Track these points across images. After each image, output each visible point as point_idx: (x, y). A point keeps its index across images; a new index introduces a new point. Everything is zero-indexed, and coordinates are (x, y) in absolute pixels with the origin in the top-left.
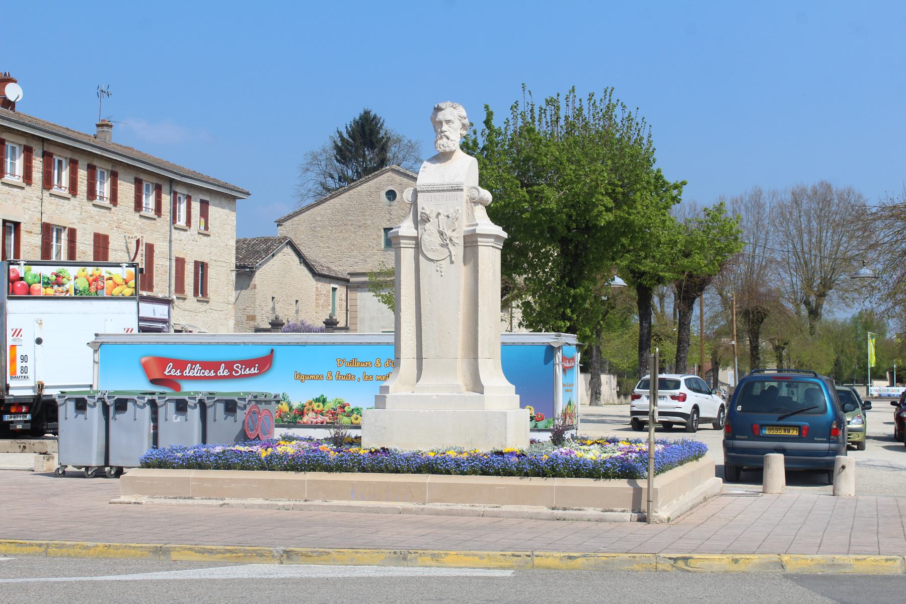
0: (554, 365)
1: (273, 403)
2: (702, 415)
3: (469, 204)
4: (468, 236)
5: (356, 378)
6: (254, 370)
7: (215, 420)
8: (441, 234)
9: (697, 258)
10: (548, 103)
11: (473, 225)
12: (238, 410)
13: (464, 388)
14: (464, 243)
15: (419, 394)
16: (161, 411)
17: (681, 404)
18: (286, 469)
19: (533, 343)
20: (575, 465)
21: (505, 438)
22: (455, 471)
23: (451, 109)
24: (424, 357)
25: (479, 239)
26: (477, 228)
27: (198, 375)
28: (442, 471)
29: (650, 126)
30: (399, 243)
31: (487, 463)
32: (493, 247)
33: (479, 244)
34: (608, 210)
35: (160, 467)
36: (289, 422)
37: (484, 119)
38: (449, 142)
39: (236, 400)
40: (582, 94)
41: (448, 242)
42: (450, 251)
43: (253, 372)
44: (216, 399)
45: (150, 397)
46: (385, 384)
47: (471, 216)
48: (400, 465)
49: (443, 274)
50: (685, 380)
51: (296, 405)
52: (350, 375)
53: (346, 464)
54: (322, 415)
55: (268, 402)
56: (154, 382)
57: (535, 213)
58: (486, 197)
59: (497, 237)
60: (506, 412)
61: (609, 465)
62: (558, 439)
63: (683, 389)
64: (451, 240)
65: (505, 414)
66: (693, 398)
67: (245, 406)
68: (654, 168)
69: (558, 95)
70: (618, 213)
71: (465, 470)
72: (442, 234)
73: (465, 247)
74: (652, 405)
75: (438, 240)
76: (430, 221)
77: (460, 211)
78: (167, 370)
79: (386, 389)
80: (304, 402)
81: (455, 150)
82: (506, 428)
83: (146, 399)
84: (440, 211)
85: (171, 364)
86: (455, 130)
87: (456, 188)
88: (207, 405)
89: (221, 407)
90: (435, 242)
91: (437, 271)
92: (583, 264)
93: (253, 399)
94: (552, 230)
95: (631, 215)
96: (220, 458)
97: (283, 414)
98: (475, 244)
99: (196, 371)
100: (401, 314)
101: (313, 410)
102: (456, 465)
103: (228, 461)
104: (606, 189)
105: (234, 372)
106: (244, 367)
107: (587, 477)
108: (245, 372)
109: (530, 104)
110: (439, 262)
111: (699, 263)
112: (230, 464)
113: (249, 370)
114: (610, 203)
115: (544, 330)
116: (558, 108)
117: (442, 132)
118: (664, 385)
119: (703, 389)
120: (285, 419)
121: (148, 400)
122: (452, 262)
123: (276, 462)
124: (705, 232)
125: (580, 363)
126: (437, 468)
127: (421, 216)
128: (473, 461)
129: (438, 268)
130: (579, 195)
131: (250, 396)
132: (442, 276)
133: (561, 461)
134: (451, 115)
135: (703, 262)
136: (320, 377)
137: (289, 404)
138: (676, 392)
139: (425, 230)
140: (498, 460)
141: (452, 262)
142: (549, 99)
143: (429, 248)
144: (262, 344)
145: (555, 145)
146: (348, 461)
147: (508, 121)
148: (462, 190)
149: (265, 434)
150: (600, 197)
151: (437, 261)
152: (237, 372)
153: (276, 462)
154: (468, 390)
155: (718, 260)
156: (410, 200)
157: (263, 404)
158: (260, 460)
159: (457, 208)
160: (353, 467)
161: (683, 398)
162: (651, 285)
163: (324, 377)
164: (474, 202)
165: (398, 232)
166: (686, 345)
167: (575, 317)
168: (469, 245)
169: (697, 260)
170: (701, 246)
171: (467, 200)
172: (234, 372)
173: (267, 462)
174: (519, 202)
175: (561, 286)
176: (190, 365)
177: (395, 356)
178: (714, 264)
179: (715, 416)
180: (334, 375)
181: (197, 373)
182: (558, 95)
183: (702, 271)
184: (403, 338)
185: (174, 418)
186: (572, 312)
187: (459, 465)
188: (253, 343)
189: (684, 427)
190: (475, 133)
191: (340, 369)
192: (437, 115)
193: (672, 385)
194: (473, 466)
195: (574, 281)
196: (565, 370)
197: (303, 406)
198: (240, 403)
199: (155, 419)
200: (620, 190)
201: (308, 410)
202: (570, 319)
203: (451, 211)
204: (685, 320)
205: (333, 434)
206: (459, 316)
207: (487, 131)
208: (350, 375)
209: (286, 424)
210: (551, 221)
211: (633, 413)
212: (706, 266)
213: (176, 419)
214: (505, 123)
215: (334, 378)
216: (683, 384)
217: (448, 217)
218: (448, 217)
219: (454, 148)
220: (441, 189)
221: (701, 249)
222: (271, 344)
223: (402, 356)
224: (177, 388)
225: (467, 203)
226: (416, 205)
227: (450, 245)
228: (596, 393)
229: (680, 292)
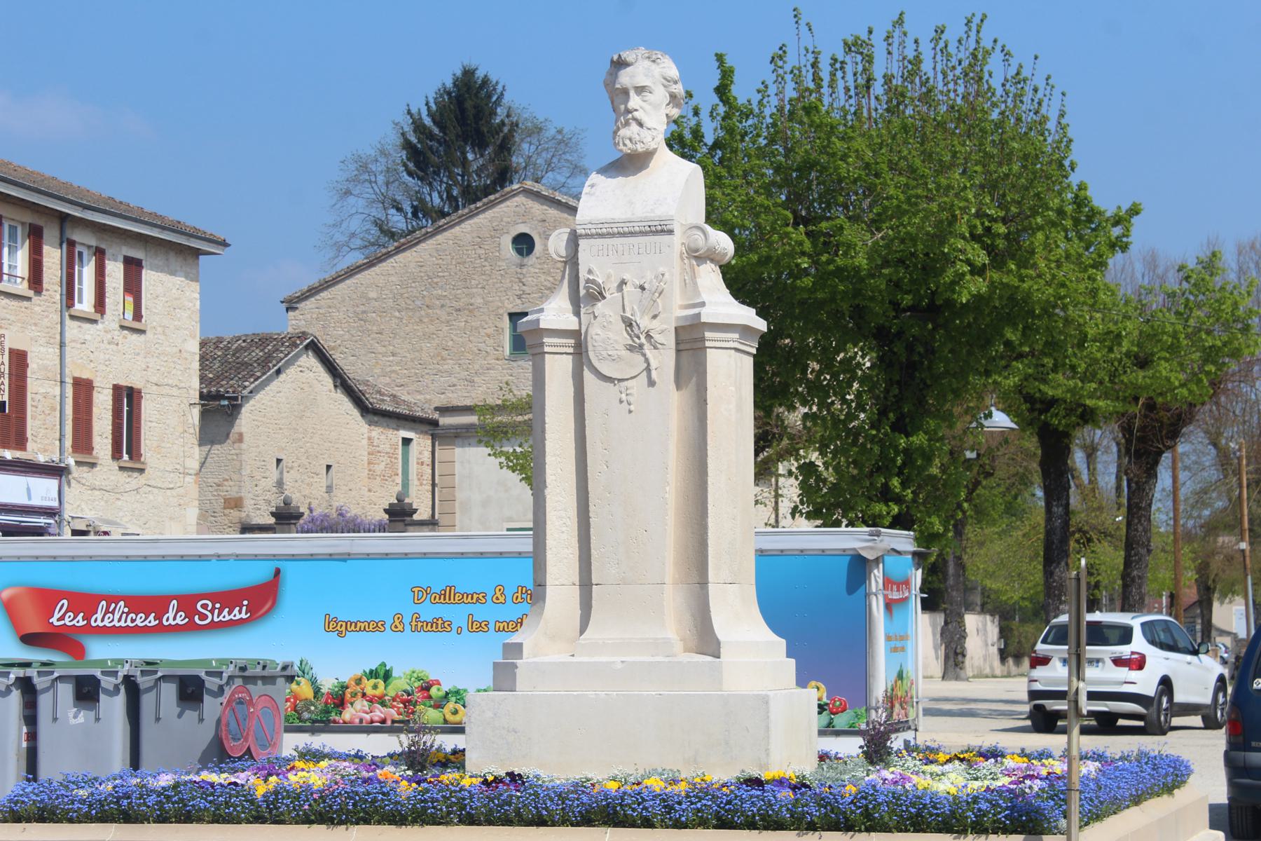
0: (867, 595)
1: (281, 681)
2: (1179, 697)
3: (686, 261)
4: (683, 327)
5: (454, 626)
6: (240, 612)
7: (158, 719)
8: (629, 324)
9: (1164, 368)
10: (848, 47)
12: (206, 698)
13: (678, 646)
14: (677, 343)
15: (585, 659)
16: (44, 701)
17: (1134, 675)
18: (307, 821)
19: (823, 551)
20: (913, 805)
21: (767, 750)
22: (662, 821)
23: (647, 63)
24: (594, 581)
25: (708, 335)
26: (704, 311)
27: (122, 624)
28: (635, 821)
29: (1063, 94)
30: (542, 344)
31: (729, 802)
32: (737, 350)
33: (708, 344)
34: (978, 271)
35: (41, 819)
36: (314, 721)
37: (717, 83)
38: (644, 132)
39: (203, 675)
40: (920, 28)
41: (643, 340)
42: (647, 361)
43: (238, 617)
44: (160, 674)
45: (20, 672)
46: (515, 638)
47: (691, 284)
48: (546, 809)
49: (632, 407)
50: (1143, 625)
51: (328, 684)
52: (440, 622)
53: (434, 808)
54: (383, 704)
55: (269, 680)
56: (29, 639)
57: (823, 278)
59: (745, 330)
60: (767, 696)
61: (984, 806)
62: (876, 751)
63: (1139, 644)
64: (649, 337)
65: (765, 700)
66: (1160, 662)
67: (221, 689)
68: (1074, 179)
69: (870, 32)
70: (996, 276)
71: (683, 819)
73: (678, 351)
74: (1074, 679)
75: (624, 338)
76: (604, 298)
77: (667, 276)
78: (57, 616)
79: (517, 649)
80: (345, 679)
81: (655, 150)
82: (767, 729)
83: (12, 676)
84: (626, 277)
85: (65, 602)
86: (656, 107)
87: (659, 228)
88: (142, 687)
89: (169, 692)
90: (616, 341)
91: (621, 402)
92: (925, 383)
93: (237, 673)
94: (859, 313)
95: (1024, 281)
96: (168, 798)
97: (300, 704)
98: (699, 345)
99: (117, 616)
100: (547, 492)
101: (364, 695)
102: (665, 807)
103: (185, 805)
104: (972, 228)
105: (197, 617)
106: (218, 605)
107: (939, 831)
108: (221, 618)
109: (810, 51)
110: (625, 383)
111: (1168, 379)
112: (189, 812)
113: (230, 613)
114: (982, 258)
115: (845, 522)
116: (869, 59)
117: (628, 111)
118: (1099, 634)
119: (1181, 645)
120: (306, 715)
121: (17, 679)
122: (651, 383)
123: (287, 806)
124: (1181, 314)
125: (922, 591)
126: (625, 815)
127: (585, 288)
128: (700, 799)
129: (623, 396)
130: (914, 239)
131: (232, 667)
132: (630, 412)
133: (883, 797)
134: (646, 76)
135: (1177, 378)
136: (377, 627)
137: (313, 682)
138: (1124, 650)
139: (595, 317)
140: (751, 796)
141: (651, 383)
142: (850, 40)
143: (604, 353)
144: (256, 557)
145: (863, 135)
146: (437, 800)
147: (766, 87)
148: (671, 232)
149: (264, 747)
150: (960, 244)
151: (620, 380)
152: (203, 617)
153: (287, 806)
154: (687, 650)
155: (1208, 373)
156: (563, 253)
157: (260, 682)
158: (252, 802)
159: (661, 269)
160: (449, 813)
161: (1138, 663)
162: (1067, 425)
163: (388, 626)
164: (696, 258)
165: (538, 321)
166: (1143, 551)
167: (909, 494)
168: (688, 346)
169: (1164, 373)
170: (1172, 344)
171: (682, 253)
172: (197, 617)
173: (268, 807)
174: (791, 255)
175: (878, 431)
176: (104, 603)
177: (535, 581)
178: (1200, 381)
179: (1207, 699)
180: (406, 621)
181: (119, 620)
182: (870, 32)
183: (1175, 398)
184: (550, 542)
185: (71, 715)
186: (904, 485)
187: (669, 809)
188: (237, 556)
189: (1141, 723)
190: (696, 113)
191: (418, 608)
192: (616, 77)
193: (1114, 635)
194: (699, 810)
195: (907, 420)
196: (889, 605)
197: (342, 687)
198: (212, 683)
199: (31, 718)
200: (1002, 229)
201: (354, 695)
202: (899, 500)
203: (649, 276)
204: (1141, 500)
205: (406, 745)
206: (667, 496)
207: (722, 109)
208: (440, 622)
209: (308, 724)
210: (857, 293)
211: (1034, 695)
212: (1182, 385)
213: (76, 718)
214: (759, 91)
215: (408, 627)
216: (1137, 634)
217: (642, 288)
218: (642, 288)
219: (653, 146)
220: (626, 230)
221: (1174, 349)
222: (274, 557)
223: (550, 580)
224: (78, 651)
225: (682, 259)
227: (647, 347)
228: (956, 654)
229: (1129, 442)
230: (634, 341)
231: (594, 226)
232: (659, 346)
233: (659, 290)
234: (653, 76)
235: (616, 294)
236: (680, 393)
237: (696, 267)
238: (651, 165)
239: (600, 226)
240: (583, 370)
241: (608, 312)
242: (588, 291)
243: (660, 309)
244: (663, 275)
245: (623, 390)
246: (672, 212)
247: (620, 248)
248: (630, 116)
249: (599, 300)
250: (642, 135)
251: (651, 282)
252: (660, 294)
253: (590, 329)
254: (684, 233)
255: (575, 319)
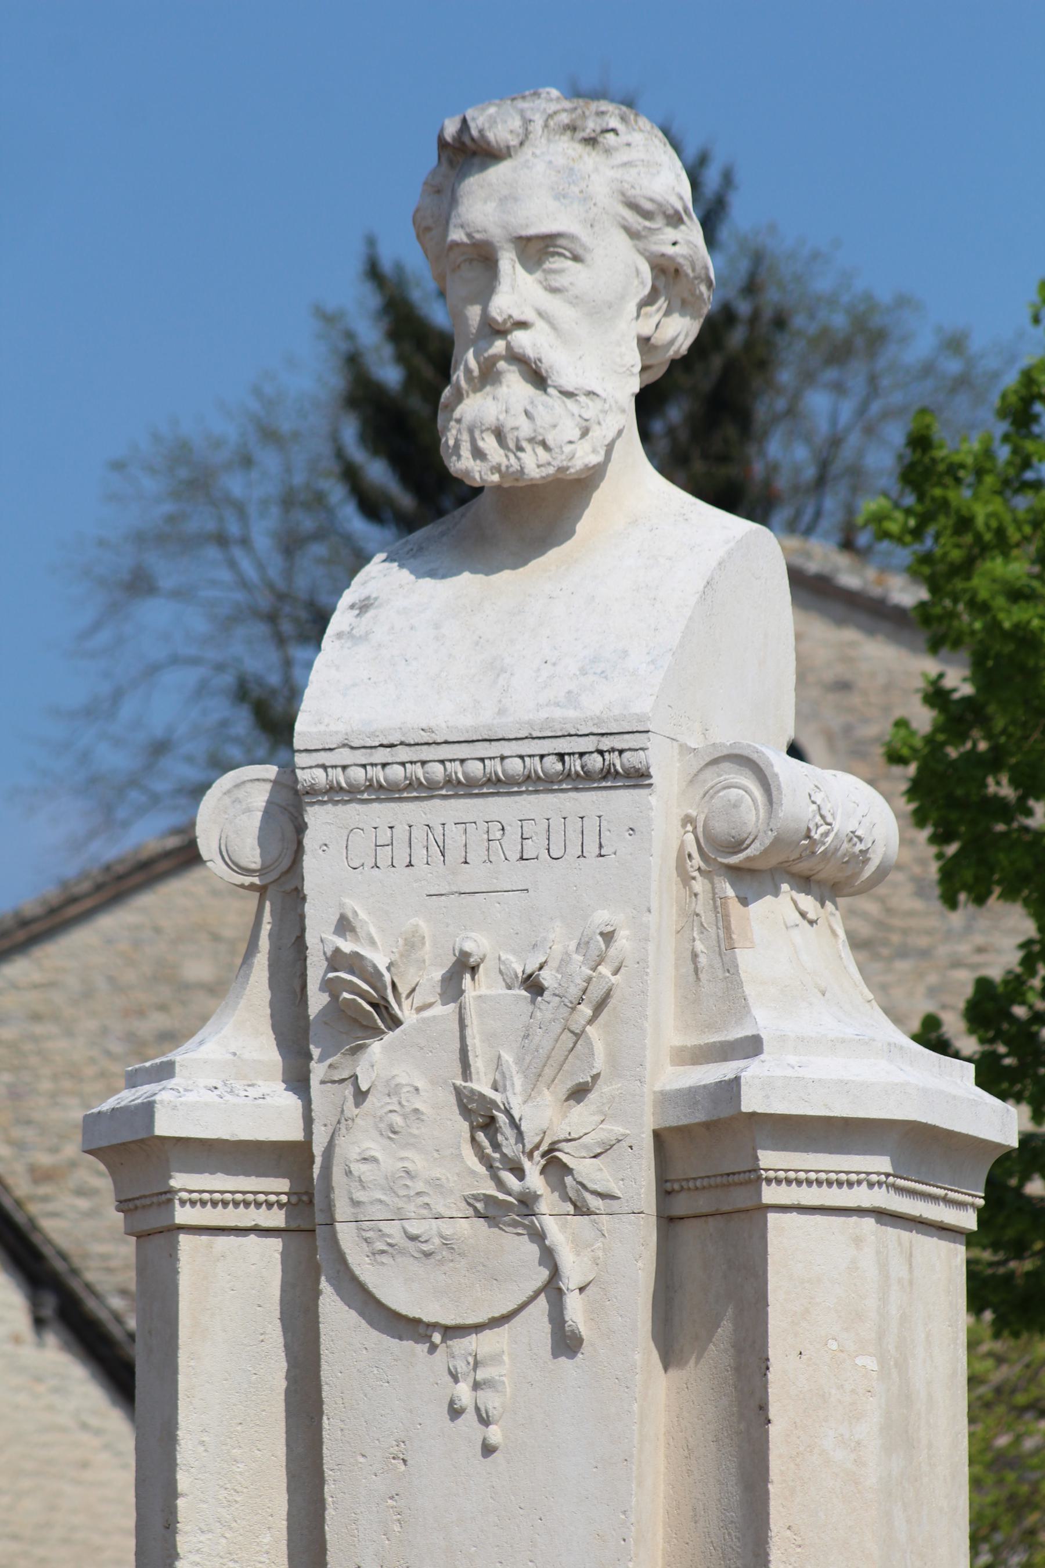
3: (699, 885)
4: (683, 1131)
11: (726, 1051)
14: (665, 1191)
23: (566, 148)
25: (769, 1159)
32: (883, 1216)
33: (770, 1194)
41: (535, 1180)
42: (549, 1257)
49: (495, 1434)
58: (842, 825)
72: (489, 1125)
76: (395, 1022)
77: (623, 941)
84: (476, 944)
87: (596, 762)
90: (436, 1184)
91: (455, 1412)
98: (739, 1198)
117: (494, 330)
127: (330, 986)
129: (464, 1392)
132: (488, 1450)
134: (560, 196)
139: (361, 1096)
143: (393, 1230)
151: (452, 1331)
156: (251, 855)
159: (602, 917)
164: (735, 872)
165: (148, 1109)
168: (702, 1203)
171: (684, 856)
192: (453, 201)
217: (533, 986)
218: (533, 986)
219: (585, 456)
220: (476, 769)
225: (686, 879)
226: (297, 897)
227: (548, 1203)
230: (500, 1184)
231: (361, 757)
232: (594, 1202)
233: (595, 993)
234: (585, 198)
235: (438, 1010)
236: (672, 1372)
237: (734, 906)
238: (580, 527)
239: (381, 756)
240: (317, 1293)
241: (406, 1074)
242: (335, 997)
243: (599, 1063)
244: (608, 937)
245: (461, 1367)
246: (643, 706)
247: (455, 836)
248: (499, 346)
249: (377, 1033)
250: (542, 416)
251: (565, 961)
252: (599, 1007)
253: (340, 1141)
254: (693, 780)
255: (292, 1102)
